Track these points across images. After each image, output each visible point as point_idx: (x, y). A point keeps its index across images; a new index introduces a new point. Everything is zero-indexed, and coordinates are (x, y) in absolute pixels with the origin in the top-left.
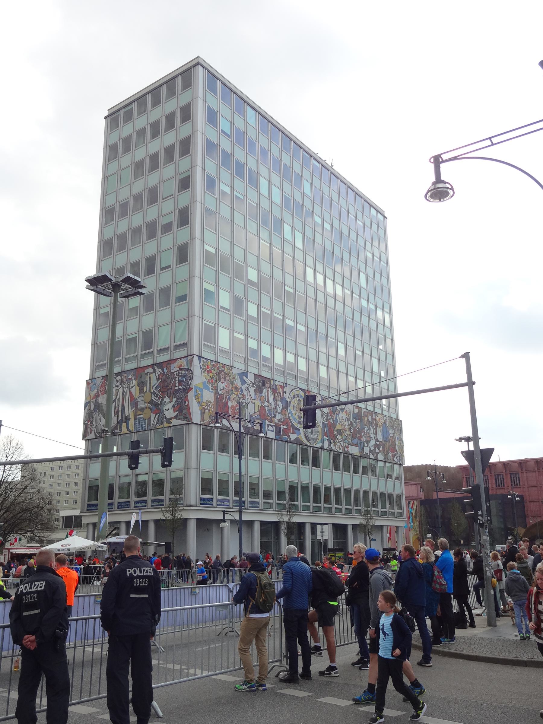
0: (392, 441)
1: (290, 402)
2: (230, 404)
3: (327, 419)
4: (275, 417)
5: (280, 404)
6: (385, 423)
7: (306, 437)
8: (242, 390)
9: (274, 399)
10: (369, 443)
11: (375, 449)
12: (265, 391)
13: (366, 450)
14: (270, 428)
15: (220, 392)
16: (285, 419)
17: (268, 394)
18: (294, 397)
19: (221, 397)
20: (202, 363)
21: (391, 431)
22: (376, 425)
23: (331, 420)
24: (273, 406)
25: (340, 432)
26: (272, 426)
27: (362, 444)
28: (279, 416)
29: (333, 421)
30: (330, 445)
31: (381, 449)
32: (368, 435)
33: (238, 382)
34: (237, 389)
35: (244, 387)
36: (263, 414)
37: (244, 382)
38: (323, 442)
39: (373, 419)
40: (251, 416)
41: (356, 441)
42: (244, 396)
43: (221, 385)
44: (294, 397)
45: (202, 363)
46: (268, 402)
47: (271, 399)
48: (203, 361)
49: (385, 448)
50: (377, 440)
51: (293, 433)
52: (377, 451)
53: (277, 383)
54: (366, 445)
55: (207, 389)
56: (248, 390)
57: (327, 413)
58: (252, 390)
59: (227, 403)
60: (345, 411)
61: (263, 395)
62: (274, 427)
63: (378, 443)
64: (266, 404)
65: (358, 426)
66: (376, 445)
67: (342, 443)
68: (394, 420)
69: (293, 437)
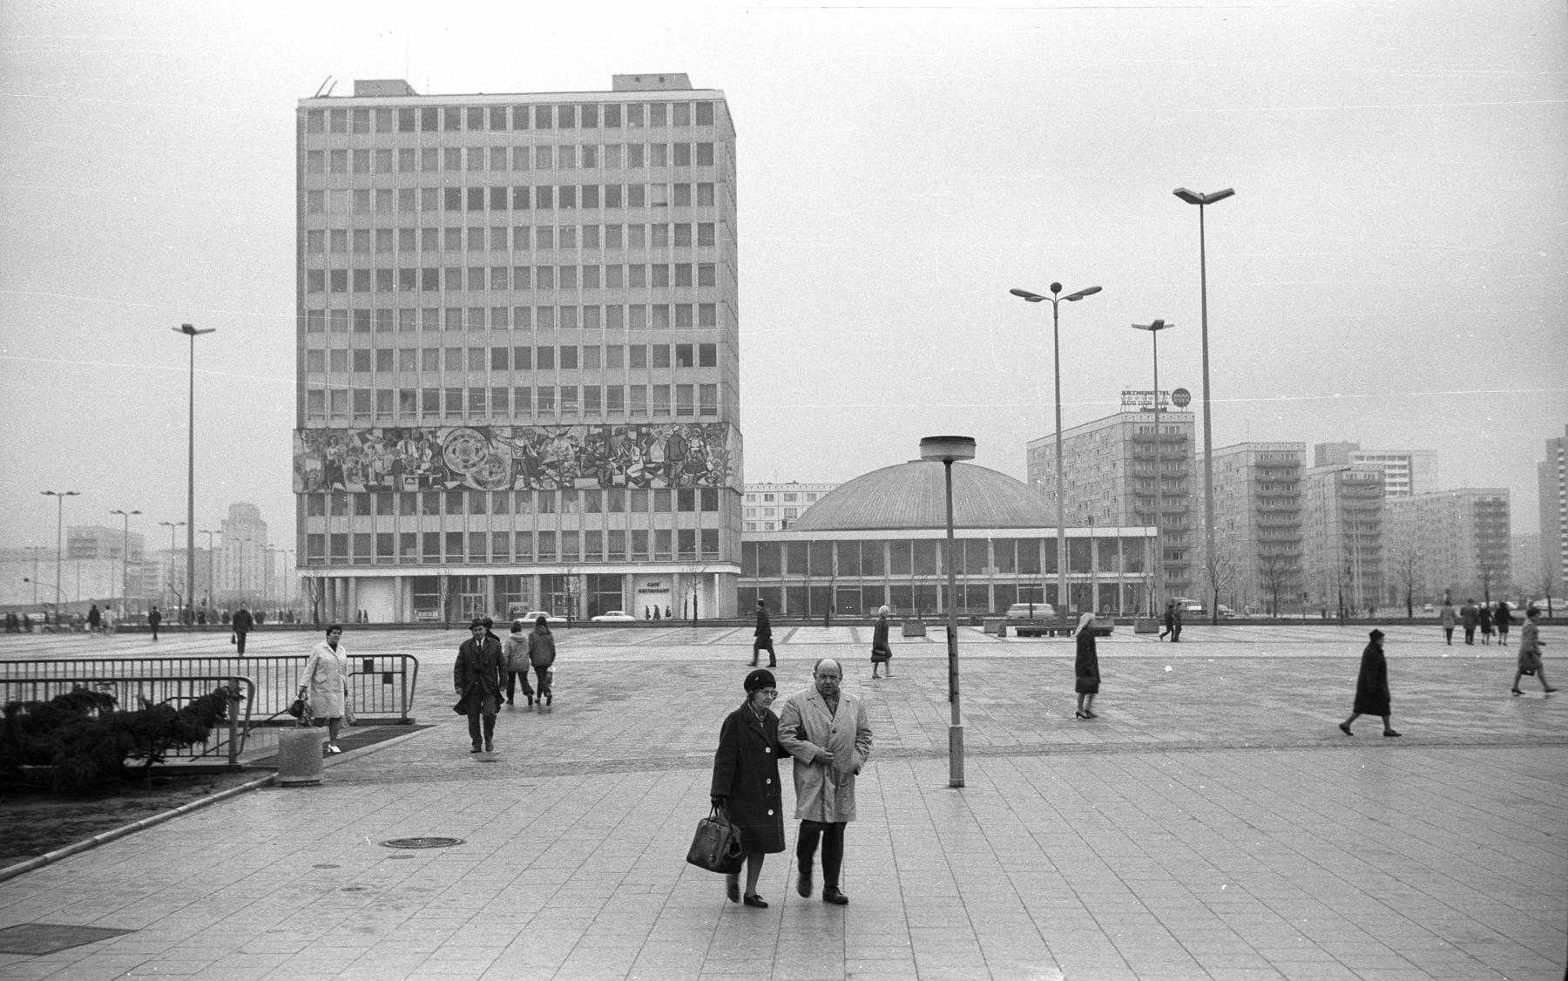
0: (697, 458)
1: (448, 446)
2: (345, 467)
3: (525, 453)
4: (418, 467)
5: (428, 452)
6: (677, 435)
7: (478, 482)
8: (363, 450)
9: (417, 448)
10: (627, 469)
11: (642, 476)
12: (401, 443)
13: (619, 479)
14: (409, 480)
15: (330, 458)
16: (435, 468)
17: (406, 444)
18: (455, 439)
19: (333, 462)
20: (304, 435)
21: (695, 444)
22: (650, 443)
23: (535, 455)
24: (416, 455)
25: (551, 465)
26: (413, 479)
27: (608, 474)
28: (425, 466)
29: (538, 453)
30: (527, 484)
31: (662, 471)
32: (625, 458)
33: (357, 442)
34: (354, 450)
35: (366, 446)
36: (397, 468)
37: (364, 440)
38: (513, 483)
39: (640, 434)
40: (377, 474)
41: (592, 470)
42: (367, 455)
43: (331, 451)
44: (455, 439)
45: (304, 435)
46: (407, 452)
47: (413, 449)
48: (307, 434)
49: (673, 473)
50: (651, 462)
51: (451, 480)
52: (648, 476)
53: (423, 430)
54: (617, 472)
55: (314, 458)
56: (373, 447)
57: (525, 447)
58: (379, 447)
59: (341, 466)
60: (568, 435)
61: (398, 447)
62: (417, 480)
63: (653, 465)
64: (403, 456)
65: (602, 450)
66: (645, 469)
67: (557, 479)
68: (704, 426)
69: (450, 485)
